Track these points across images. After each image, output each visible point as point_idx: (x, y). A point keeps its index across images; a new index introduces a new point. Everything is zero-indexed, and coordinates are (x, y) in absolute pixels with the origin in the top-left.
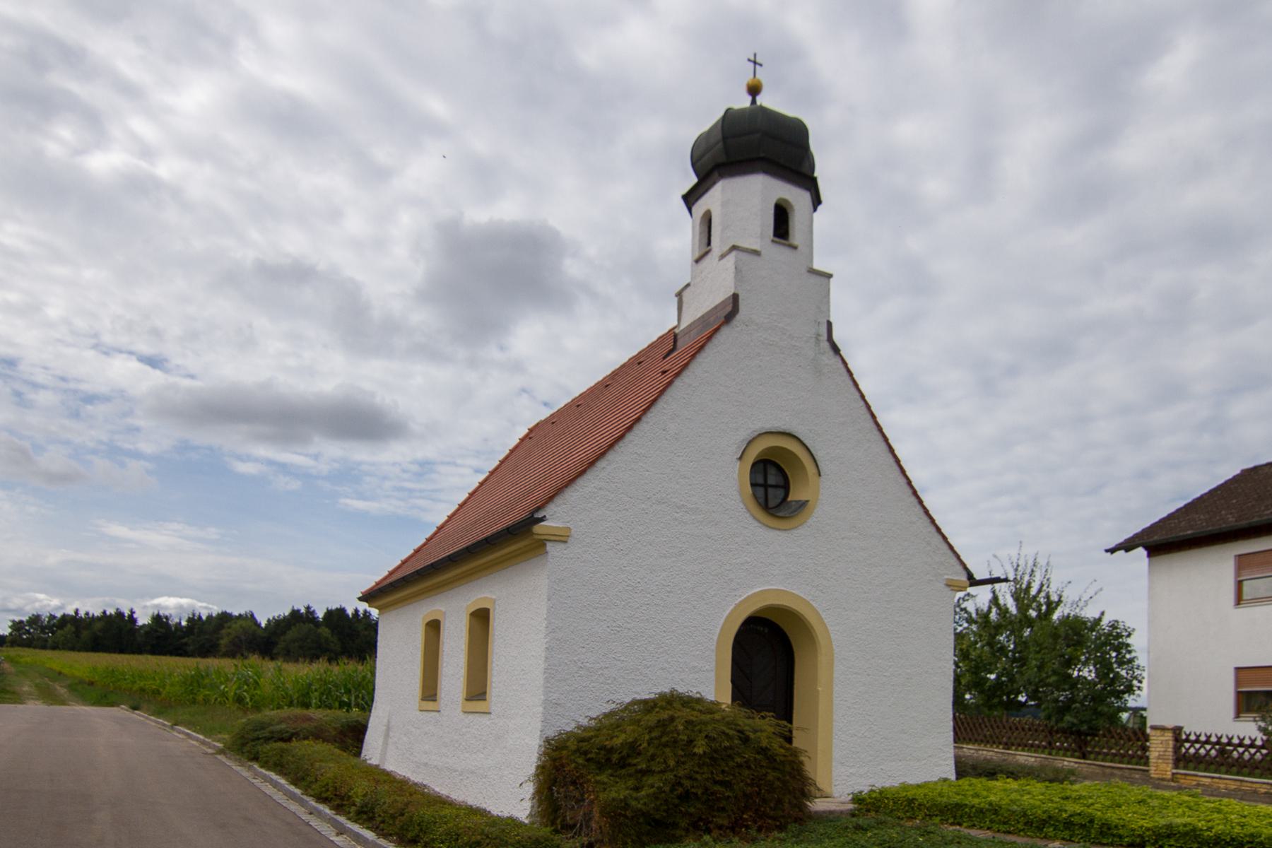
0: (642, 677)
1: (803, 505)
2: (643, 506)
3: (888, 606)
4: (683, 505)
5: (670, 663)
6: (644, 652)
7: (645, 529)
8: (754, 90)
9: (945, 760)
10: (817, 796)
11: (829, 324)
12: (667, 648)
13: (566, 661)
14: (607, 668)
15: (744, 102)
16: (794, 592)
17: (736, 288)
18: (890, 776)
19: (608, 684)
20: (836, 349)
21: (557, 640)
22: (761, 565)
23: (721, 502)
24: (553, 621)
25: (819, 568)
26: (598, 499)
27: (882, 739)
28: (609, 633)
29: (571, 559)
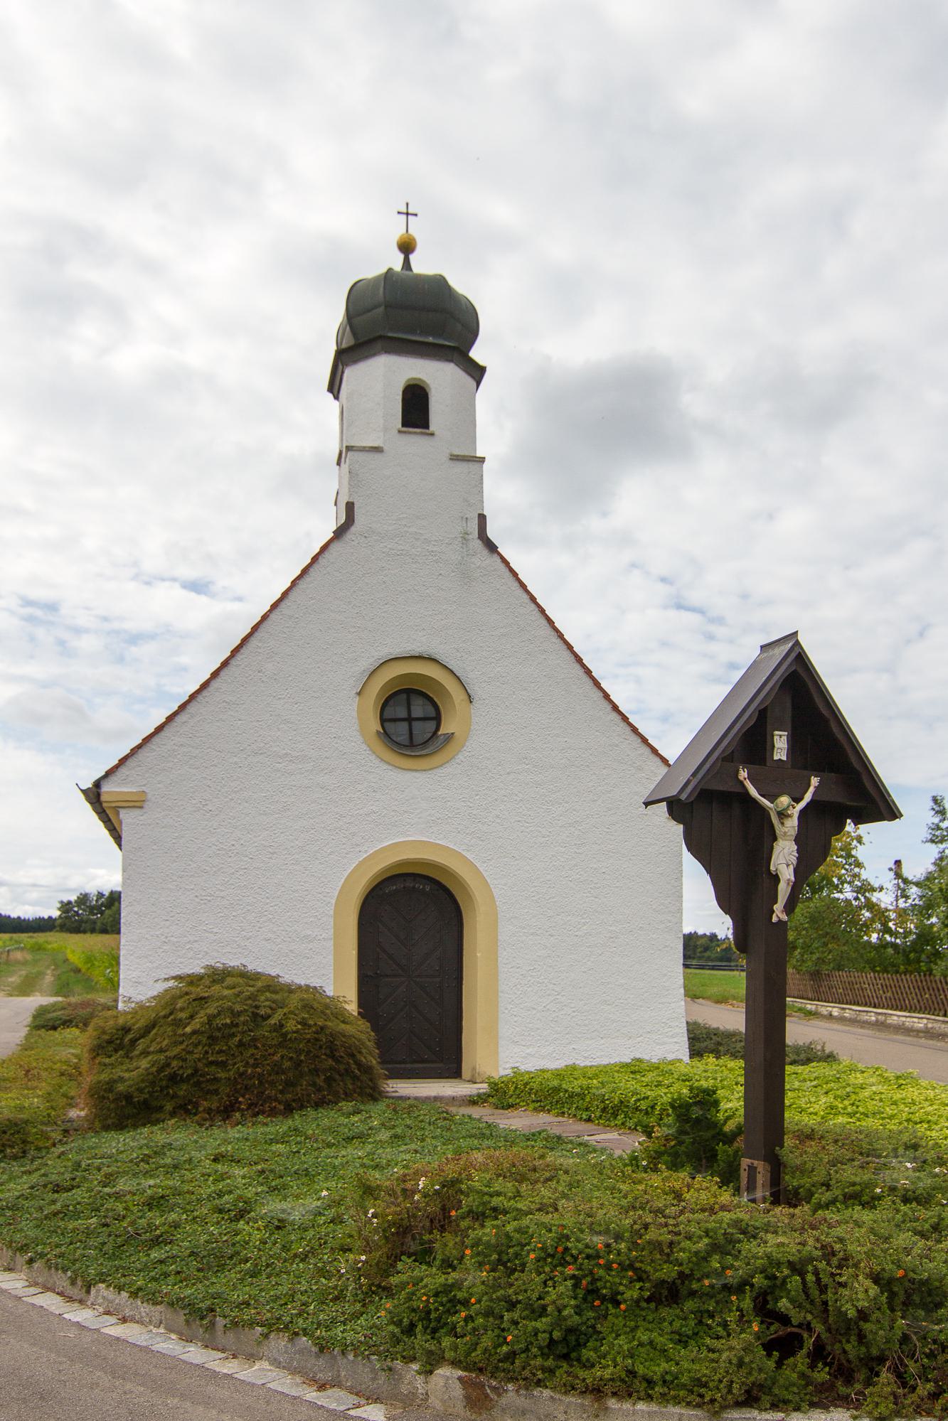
0: (240, 950)
1: (449, 737)
2: (235, 759)
3: (580, 851)
4: (286, 754)
5: (275, 932)
6: (242, 922)
7: (239, 785)
8: (407, 247)
9: (672, 1037)
10: (478, 1081)
11: (482, 519)
12: (271, 917)
13: (147, 936)
14: (196, 941)
15: (397, 263)
16: (440, 842)
17: (350, 497)
18: (585, 1058)
19: (199, 959)
20: (491, 547)
21: (136, 913)
22: (393, 813)
23: (336, 745)
24: (130, 893)
25: (475, 812)
26: (179, 756)
27: (574, 1012)
28: (199, 903)
29: (150, 825)
